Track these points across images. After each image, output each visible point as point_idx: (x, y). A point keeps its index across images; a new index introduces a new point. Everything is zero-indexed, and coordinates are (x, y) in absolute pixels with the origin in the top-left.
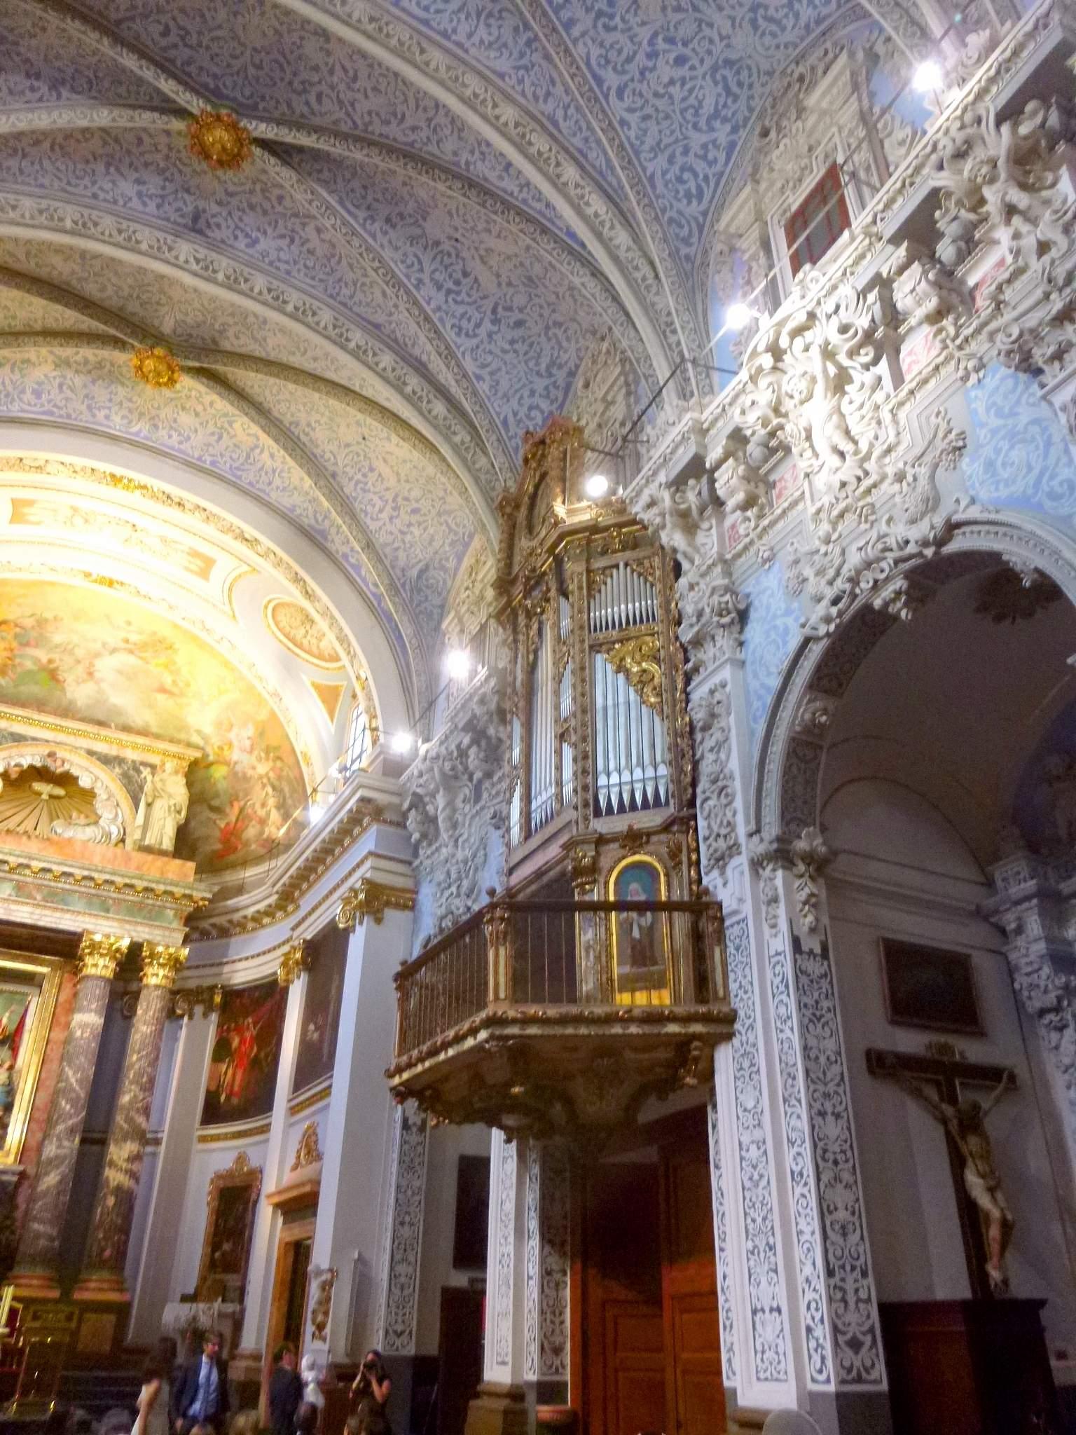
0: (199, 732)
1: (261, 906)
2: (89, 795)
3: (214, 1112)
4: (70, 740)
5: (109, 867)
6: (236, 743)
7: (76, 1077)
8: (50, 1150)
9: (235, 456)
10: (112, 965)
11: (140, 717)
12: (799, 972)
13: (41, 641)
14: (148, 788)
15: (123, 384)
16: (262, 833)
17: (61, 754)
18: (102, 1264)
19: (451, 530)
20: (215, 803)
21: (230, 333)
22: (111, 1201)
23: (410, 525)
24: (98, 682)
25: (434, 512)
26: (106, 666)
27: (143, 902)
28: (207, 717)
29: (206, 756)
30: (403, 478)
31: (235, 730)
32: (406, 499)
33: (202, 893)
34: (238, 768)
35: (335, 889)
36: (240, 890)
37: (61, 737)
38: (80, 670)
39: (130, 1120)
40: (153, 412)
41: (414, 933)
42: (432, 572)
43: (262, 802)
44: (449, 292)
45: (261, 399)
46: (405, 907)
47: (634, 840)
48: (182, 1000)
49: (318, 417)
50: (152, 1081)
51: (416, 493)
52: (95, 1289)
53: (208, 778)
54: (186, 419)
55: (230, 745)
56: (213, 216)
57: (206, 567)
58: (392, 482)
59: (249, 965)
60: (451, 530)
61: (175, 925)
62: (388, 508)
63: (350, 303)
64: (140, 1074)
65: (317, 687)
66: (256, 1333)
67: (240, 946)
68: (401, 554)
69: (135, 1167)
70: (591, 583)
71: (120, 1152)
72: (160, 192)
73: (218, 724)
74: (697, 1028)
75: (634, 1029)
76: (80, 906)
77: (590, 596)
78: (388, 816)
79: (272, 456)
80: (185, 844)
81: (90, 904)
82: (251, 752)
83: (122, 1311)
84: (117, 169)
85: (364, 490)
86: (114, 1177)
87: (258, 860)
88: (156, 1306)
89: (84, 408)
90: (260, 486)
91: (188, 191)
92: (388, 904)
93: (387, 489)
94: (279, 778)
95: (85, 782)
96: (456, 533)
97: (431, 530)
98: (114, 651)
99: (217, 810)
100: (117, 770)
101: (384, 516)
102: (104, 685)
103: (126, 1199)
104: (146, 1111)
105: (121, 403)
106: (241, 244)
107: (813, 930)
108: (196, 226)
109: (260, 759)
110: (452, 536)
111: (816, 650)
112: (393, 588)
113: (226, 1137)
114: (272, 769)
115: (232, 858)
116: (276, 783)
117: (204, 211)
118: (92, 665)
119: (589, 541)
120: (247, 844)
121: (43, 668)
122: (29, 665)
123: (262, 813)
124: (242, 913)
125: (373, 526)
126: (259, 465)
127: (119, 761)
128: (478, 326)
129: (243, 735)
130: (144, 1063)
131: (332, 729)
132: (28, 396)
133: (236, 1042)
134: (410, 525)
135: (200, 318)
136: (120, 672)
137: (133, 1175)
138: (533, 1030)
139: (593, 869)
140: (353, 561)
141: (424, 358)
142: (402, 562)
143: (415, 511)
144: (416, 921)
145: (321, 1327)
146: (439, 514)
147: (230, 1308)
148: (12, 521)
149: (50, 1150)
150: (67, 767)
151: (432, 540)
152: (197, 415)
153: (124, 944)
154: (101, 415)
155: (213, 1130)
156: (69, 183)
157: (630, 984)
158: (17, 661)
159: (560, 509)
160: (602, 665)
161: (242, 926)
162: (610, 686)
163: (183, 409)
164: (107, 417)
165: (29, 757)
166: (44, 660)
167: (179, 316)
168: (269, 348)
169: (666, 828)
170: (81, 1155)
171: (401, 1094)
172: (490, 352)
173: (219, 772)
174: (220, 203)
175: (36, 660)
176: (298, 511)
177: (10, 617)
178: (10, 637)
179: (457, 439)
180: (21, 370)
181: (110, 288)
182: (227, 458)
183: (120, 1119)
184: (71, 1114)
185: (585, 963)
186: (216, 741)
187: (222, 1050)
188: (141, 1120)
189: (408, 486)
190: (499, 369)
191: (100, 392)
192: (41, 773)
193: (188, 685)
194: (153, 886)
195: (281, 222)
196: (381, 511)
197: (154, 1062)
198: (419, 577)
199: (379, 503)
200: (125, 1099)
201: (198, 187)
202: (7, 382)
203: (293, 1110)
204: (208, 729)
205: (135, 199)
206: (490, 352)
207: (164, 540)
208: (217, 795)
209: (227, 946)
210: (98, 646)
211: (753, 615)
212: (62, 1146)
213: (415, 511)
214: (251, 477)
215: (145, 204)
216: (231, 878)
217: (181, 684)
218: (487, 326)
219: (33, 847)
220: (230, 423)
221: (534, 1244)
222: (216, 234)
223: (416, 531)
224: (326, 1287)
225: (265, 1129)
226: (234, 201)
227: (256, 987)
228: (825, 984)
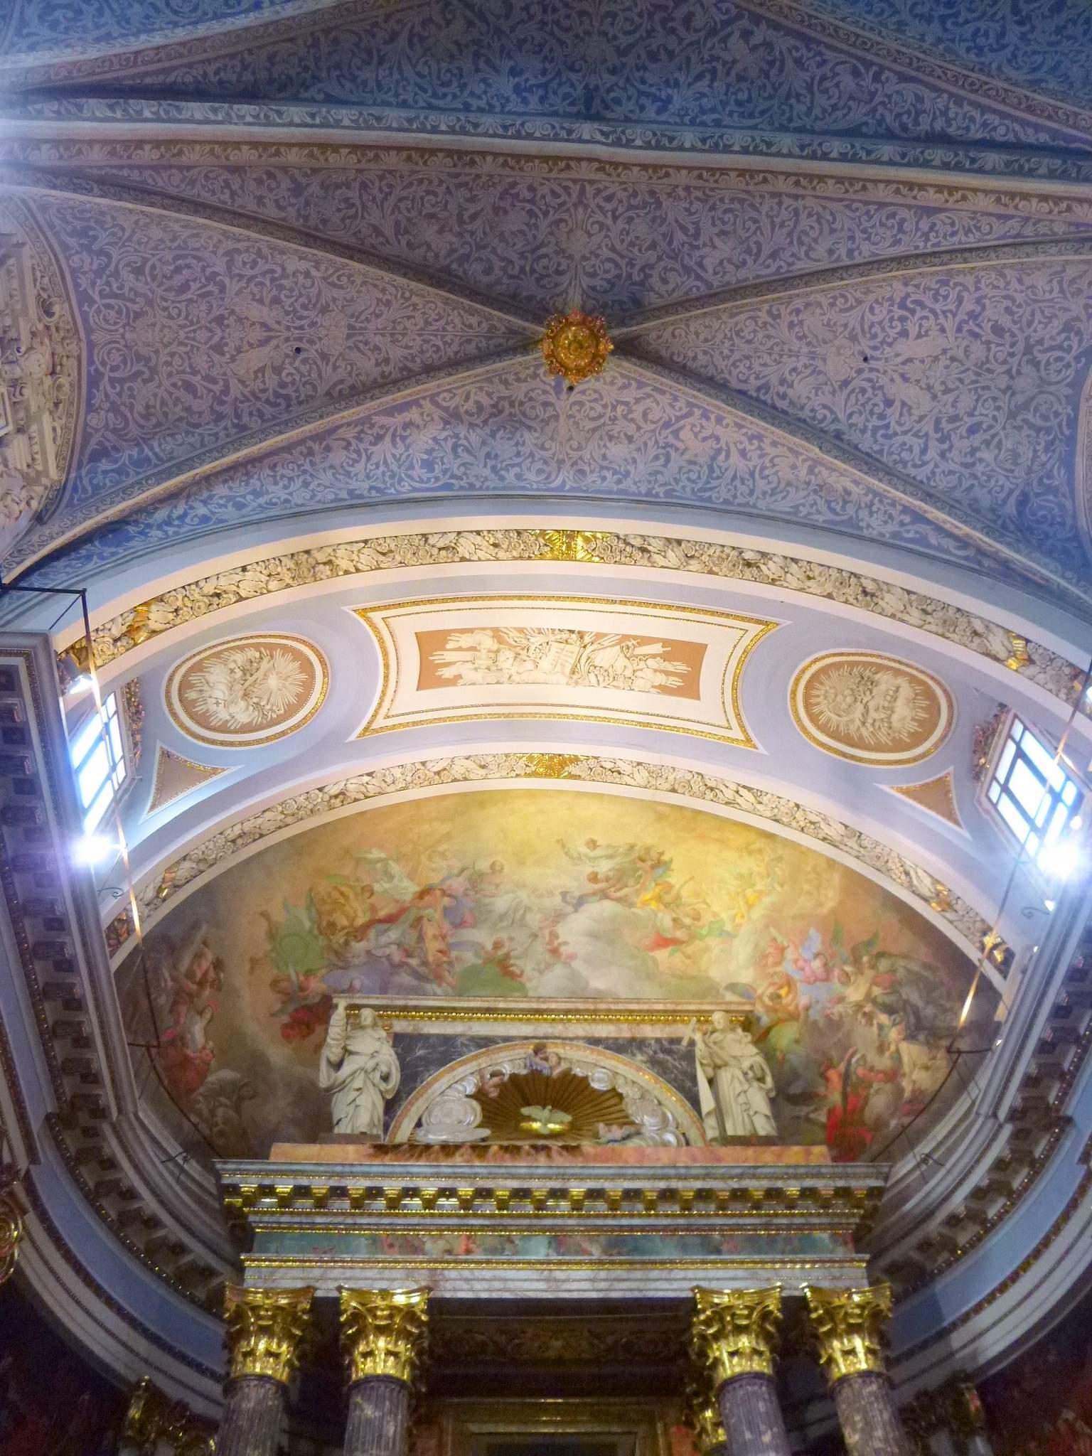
0: (732, 987)
1: (979, 1177)
6: (797, 976)
9: (694, 476)
15: (529, 428)
16: (900, 1091)
19: (1038, 430)
21: (654, 281)
23: (974, 451)
24: (567, 964)
25: (1002, 418)
26: (574, 931)
30: (938, 388)
31: (790, 955)
32: (954, 419)
34: (814, 1015)
38: (540, 948)
40: (575, 455)
42: (1035, 502)
44: (943, 19)
45: (711, 371)
49: (790, 363)
51: (967, 401)
54: (618, 451)
55: (789, 983)
56: (609, 90)
58: (924, 403)
60: (1038, 430)
61: (840, 1253)
62: (933, 444)
63: (808, 122)
65: (907, 792)
67: (953, 1291)
68: (979, 493)
72: (543, 80)
73: (760, 960)
79: (743, 453)
82: (827, 979)
84: (488, 61)
85: (884, 436)
89: (487, 472)
90: (740, 500)
91: (572, 69)
93: (921, 418)
94: (894, 987)
96: (1048, 431)
97: (1008, 444)
98: (580, 902)
100: (639, 1057)
101: (932, 454)
102: (577, 965)
105: (532, 455)
106: (651, 113)
108: (591, 107)
109: (846, 979)
110: (1043, 438)
114: (875, 983)
116: (888, 1000)
117: (597, 88)
118: (554, 936)
120: (880, 1124)
121: (489, 960)
122: (470, 958)
123: (884, 1062)
124: (941, 1215)
125: (921, 474)
126: (730, 474)
128: (1002, 34)
129: (802, 959)
131: (966, 834)
132: (418, 472)
134: (974, 451)
135: (613, 272)
136: (594, 935)
140: (911, 535)
141: (939, 124)
142: (986, 502)
143: (972, 430)
146: (1012, 415)
148: (420, 687)
150: (564, 1066)
151: (1015, 455)
152: (630, 439)
154: (510, 476)
156: (435, 95)
158: (454, 954)
163: (611, 438)
164: (519, 477)
166: (489, 946)
167: (586, 281)
168: (708, 276)
172: (1034, 53)
174: (613, 71)
175: (478, 948)
176: (804, 511)
177: (435, 879)
178: (437, 916)
179: (1043, 170)
180: (403, 438)
181: (498, 264)
182: (684, 482)
186: (764, 989)
189: (950, 397)
190: (1059, 62)
191: (504, 447)
193: (697, 918)
194: (779, 1184)
195: (694, 58)
196: (924, 451)
198: (1020, 513)
199: (917, 444)
201: (583, 59)
202: (390, 459)
204: (746, 977)
205: (514, 97)
206: (1034, 53)
213: (972, 430)
214: (724, 494)
215: (525, 101)
217: (687, 921)
218: (1013, 33)
220: (676, 434)
222: (619, 111)
223: (987, 455)
226: (630, 60)
227: (1042, 1347)
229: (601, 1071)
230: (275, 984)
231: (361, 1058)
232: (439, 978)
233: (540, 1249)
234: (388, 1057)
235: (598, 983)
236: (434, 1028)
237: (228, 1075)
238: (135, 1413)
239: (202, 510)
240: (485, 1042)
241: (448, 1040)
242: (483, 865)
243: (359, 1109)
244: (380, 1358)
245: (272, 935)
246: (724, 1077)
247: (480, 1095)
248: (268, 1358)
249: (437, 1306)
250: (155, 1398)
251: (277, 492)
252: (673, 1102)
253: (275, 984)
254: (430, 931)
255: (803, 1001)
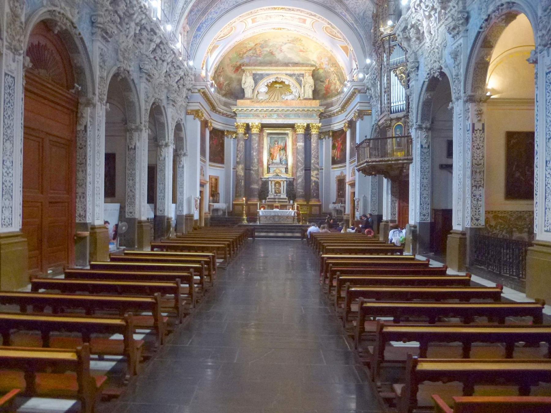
1: (337, 110)
2: (289, 86)
3: (334, 162)
4: (281, 72)
5: (298, 106)
7: (301, 157)
8: (298, 174)
10: (303, 130)
11: (297, 59)
12: (421, 152)
13: (267, 46)
14: (303, 82)
17: (279, 76)
18: (314, 197)
20: (321, 80)
22: (313, 184)
26: (284, 48)
27: (307, 114)
28: (313, 57)
29: (316, 67)
33: (322, 109)
35: (353, 109)
36: (331, 105)
37: (278, 72)
39: (314, 166)
41: (372, 121)
43: (334, 79)
46: (369, 115)
47: (398, 119)
48: (322, 134)
50: (318, 156)
52: (313, 202)
53: (318, 73)
57: (304, 21)
59: (338, 124)
64: (315, 155)
65: (342, 47)
66: (348, 210)
68: (357, 9)
69: (318, 176)
70: (390, 50)
71: (313, 173)
74: (405, 161)
75: (393, 162)
76: (293, 117)
77: (390, 55)
78: (362, 91)
80: (316, 94)
81: (295, 116)
83: (320, 206)
86: (313, 179)
87: (336, 95)
88: (327, 206)
92: (364, 115)
94: (337, 72)
95: (287, 83)
98: (286, 44)
99: (322, 82)
103: (317, 183)
104: (318, 164)
107: (426, 143)
111: (426, 83)
112: (356, 21)
113: (337, 168)
115: (329, 95)
119: (389, 38)
120: (332, 91)
122: (265, 53)
123: (334, 82)
127: (294, 75)
129: (325, 61)
130: (315, 153)
131: (348, 59)
133: (337, 145)
136: (288, 48)
137: (317, 178)
138: (374, 163)
139: (390, 126)
142: (357, 12)
144: (372, 118)
145: (358, 209)
147: (343, 205)
149: (298, 174)
153: (305, 125)
155: (335, 166)
157: (397, 150)
159: (382, 29)
160: (392, 74)
161: (334, 114)
162: (394, 79)
165: (272, 79)
169: (404, 116)
170: (305, 174)
171: (359, 170)
173: (321, 71)
175: (267, 51)
183: (312, 166)
184: (301, 166)
185: (389, 147)
187: (334, 147)
188: (317, 166)
192: (276, 82)
197: (318, 152)
200: (312, 161)
203: (351, 163)
204: (316, 60)
207: (291, 17)
208: (322, 78)
209: (331, 120)
210: (281, 44)
211: (420, 68)
212: (301, 173)
216: (329, 101)
219: (278, 104)
221: (390, 196)
224: (358, 202)
225: (345, 166)
228: (428, 154)
229: (288, 81)
230: (232, 66)
231: (248, 82)
232: (260, 56)
233: (275, 116)
234: (252, 81)
235: (289, 56)
236: (259, 72)
237: (227, 82)
238: (226, 133)
239: (210, 16)
240: (268, 75)
241: (262, 74)
242: (267, 39)
243: (248, 93)
244: (255, 131)
245: (230, 60)
246: (306, 86)
247: (267, 86)
248: (241, 131)
249: (262, 124)
250: (228, 131)
251: (222, 7)
252: (298, 86)
253: (232, 66)
254: (258, 50)
255: (324, 67)
